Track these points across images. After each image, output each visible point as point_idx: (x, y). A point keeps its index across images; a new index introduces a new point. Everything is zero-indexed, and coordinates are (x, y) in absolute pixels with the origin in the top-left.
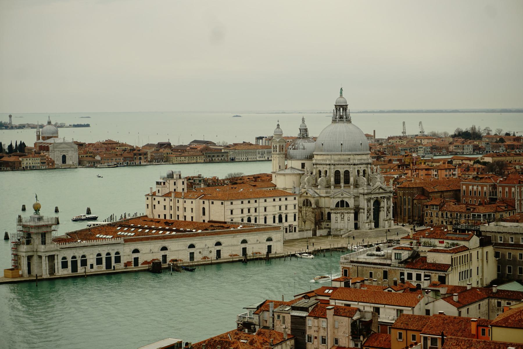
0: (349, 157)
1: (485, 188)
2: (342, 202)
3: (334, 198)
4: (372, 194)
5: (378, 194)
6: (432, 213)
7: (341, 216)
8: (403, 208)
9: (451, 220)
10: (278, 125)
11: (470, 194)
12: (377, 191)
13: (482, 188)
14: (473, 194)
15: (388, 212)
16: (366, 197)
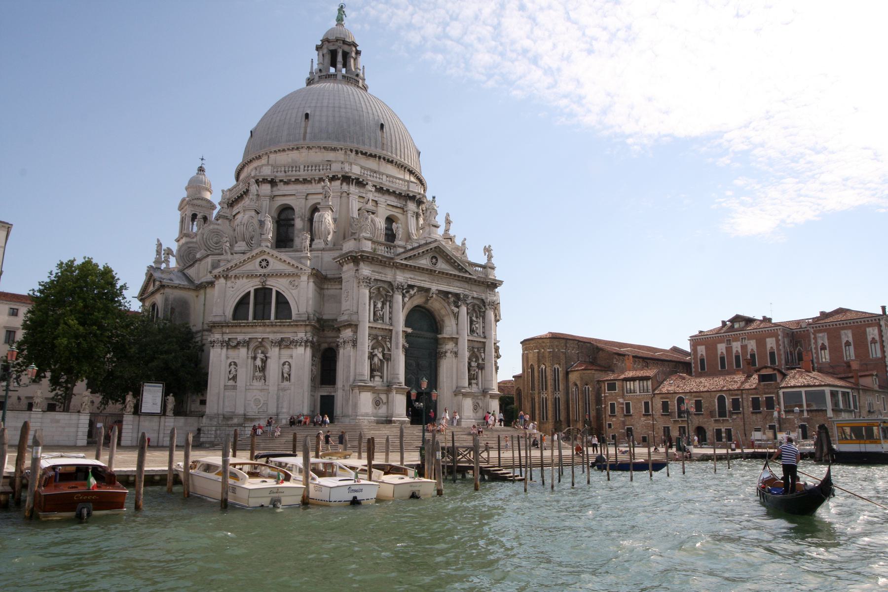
0: (331, 156)
1: (771, 343)
2: (263, 294)
3: (226, 278)
4: (397, 268)
5: (425, 277)
6: (628, 405)
7: (255, 358)
8: (539, 397)
9: (696, 421)
10: (201, 170)
11: (723, 366)
12: (425, 262)
13: (761, 343)
14: (730, 364)
15: (474, 364)
16: (366, 270)
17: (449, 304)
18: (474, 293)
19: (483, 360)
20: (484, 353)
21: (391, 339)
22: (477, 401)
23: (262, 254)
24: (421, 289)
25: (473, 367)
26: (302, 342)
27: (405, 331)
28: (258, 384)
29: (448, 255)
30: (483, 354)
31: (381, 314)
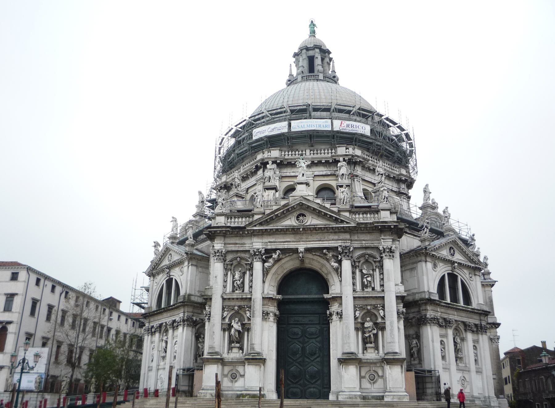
4: (255, 235)
17: (328, 260)
18: (364, 242)
19: (383, 318)
20: (384, 310)
21: (250, 307)
22: (376, 369)
23: (168, 250)
24: (284, 251)
25: (367, 328)
26: (180, 322)
27: (267, 298)
28: (162, 363)
29: (314, 209)
30: (381, 312)
31: (239, 283)
